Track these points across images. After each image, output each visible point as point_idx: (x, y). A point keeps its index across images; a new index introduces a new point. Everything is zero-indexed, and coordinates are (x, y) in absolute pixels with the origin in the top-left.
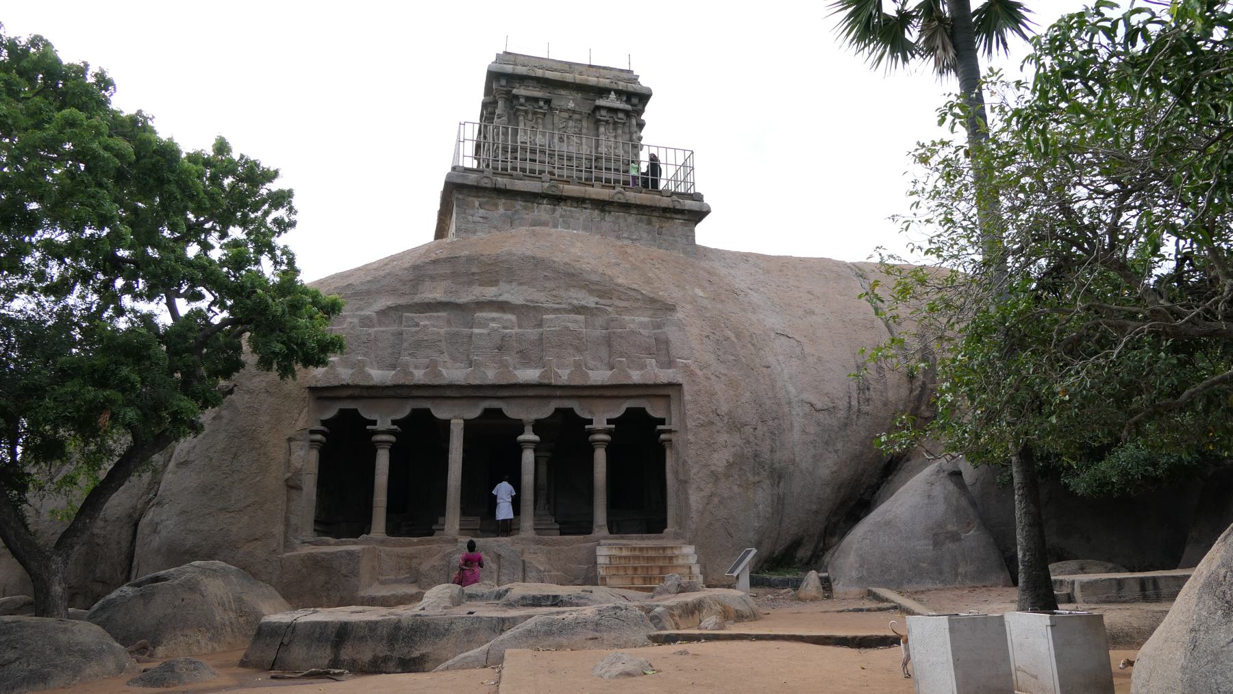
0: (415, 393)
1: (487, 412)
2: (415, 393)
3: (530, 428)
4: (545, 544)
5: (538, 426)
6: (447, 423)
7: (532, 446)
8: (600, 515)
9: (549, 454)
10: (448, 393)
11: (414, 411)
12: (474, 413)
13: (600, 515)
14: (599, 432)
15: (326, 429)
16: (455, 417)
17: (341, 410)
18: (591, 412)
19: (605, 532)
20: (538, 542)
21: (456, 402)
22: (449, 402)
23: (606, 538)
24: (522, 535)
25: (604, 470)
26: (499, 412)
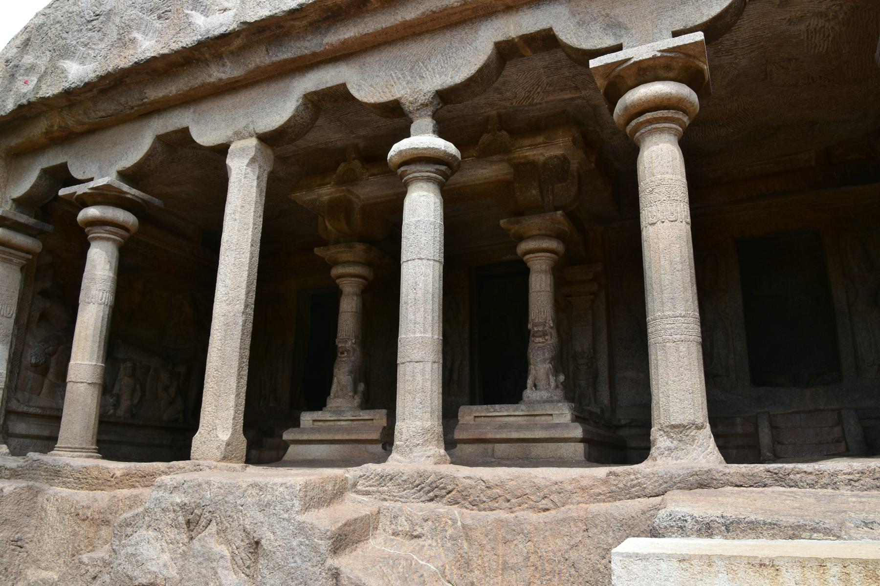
0: (154, 94)
1: (316, 102)
2: (154, 94)
3: (427, 122)
4: (460, 496)
5: (448, 109)
6: (222, 150)
7: (428, 170)
8: (678, 380)
9: (553, 244)
10: (218, 73)
11: (160, 139)
12: (279, 109)
13: (678, 380)
14: (646, 72)
15: (23, 218)
16: (239, 135)
17: (45, 171)
18: (613, 25)
19: (704, 453)
20: (434, 490)
21: (244, 97)
22: (228, 101)
23: (702, 482)
24: (396, 463)
25: (682, 210)
26: (340, 95)
